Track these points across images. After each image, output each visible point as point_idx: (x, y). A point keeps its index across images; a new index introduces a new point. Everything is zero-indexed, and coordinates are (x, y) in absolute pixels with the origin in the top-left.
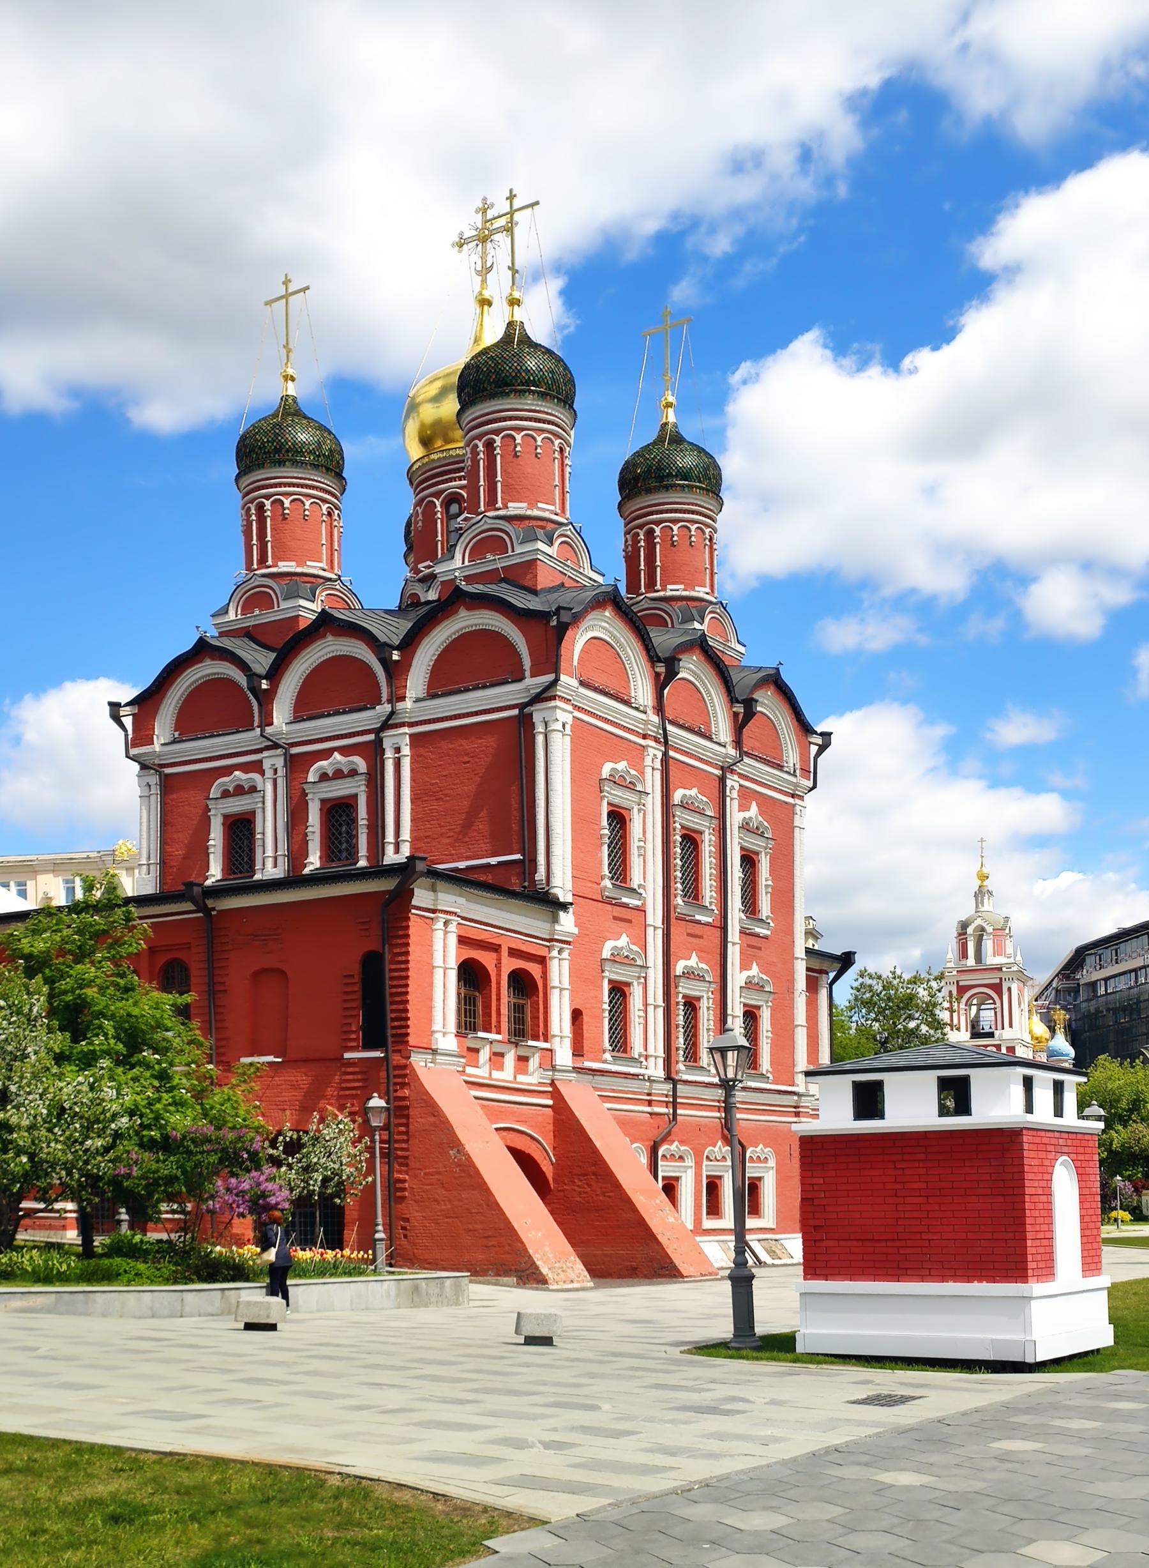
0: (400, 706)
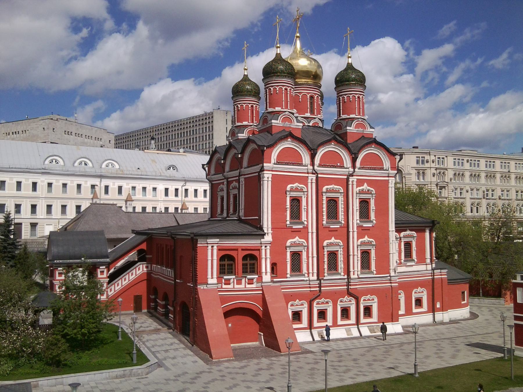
0: (242, 170)
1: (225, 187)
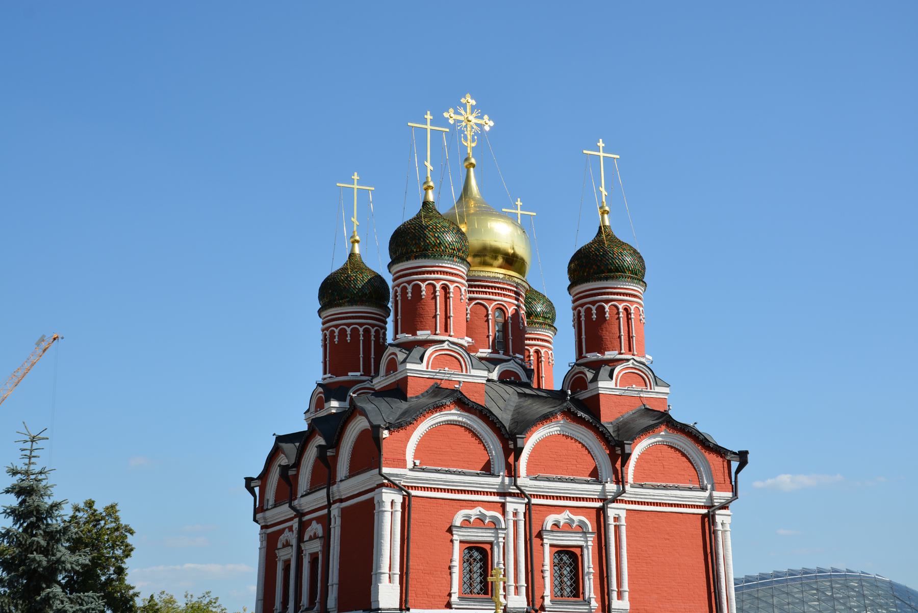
0: (334, 488)
1: (293, 538)
